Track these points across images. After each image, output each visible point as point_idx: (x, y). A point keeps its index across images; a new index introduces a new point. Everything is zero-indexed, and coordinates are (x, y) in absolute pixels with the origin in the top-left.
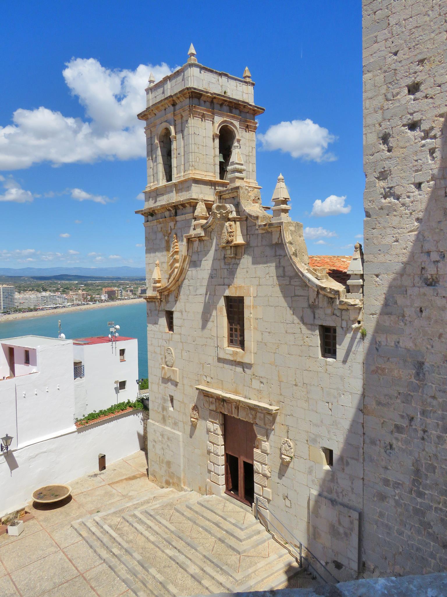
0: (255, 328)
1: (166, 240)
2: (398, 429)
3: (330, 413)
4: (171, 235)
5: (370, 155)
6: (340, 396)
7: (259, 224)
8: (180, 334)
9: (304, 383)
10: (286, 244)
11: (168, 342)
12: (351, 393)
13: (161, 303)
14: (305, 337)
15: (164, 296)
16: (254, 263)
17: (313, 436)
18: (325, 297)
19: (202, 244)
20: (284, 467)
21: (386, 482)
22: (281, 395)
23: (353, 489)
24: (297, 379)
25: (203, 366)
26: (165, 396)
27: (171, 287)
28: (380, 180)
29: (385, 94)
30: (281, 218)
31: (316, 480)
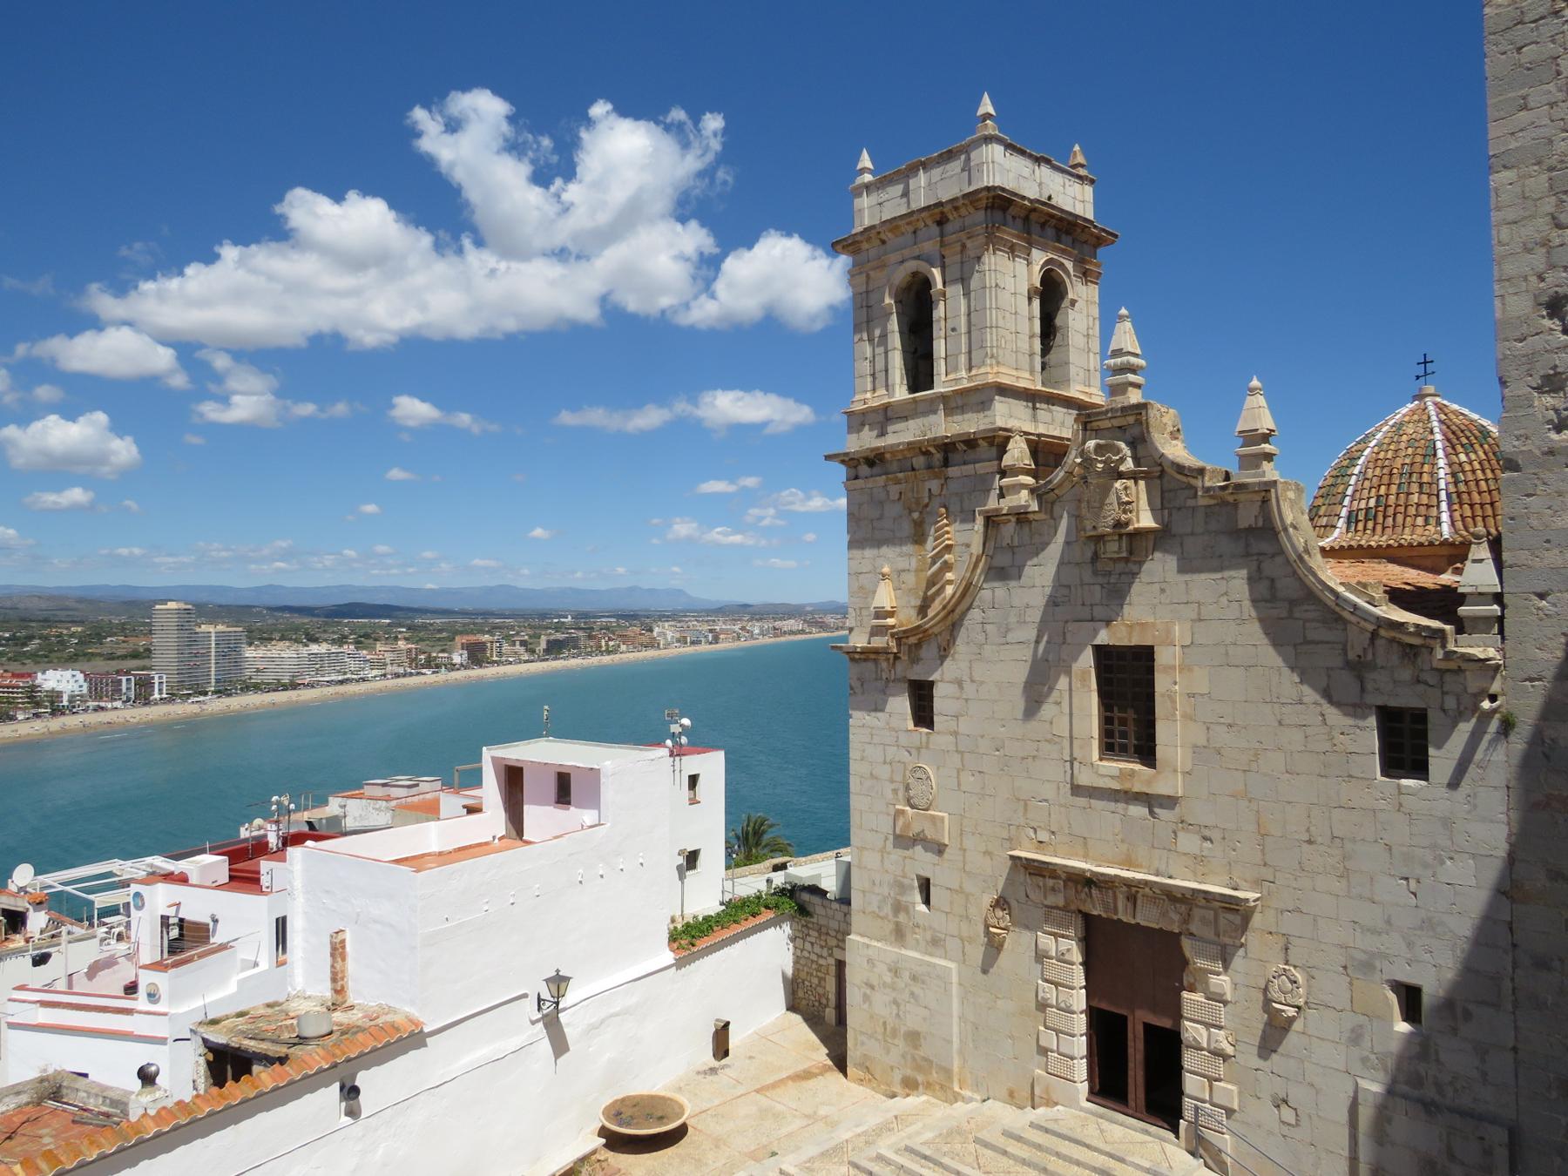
0: (1185, 716)
1: (915, 522)
3: (1413, 901)
4: (928, 509)
5: (1515, 340)
6: (1442, 863)
7: (1208, 484)
8: (955, 734)
9: (1333, 837)
10: (1285, 530)
11: (914, 752)
12: (1474, 856)
13: (894, 664)
14: (1336, 733)
15: (907, 647)
16: (1182, 570)
17: (1363, 957)
18: (1395, 645)
19: (1026, 529)
20: (1274, 1033)
22: (1265, 865)
23: (1484, 1074)
24: (1312, 828)
25: (1026, 805)
26: (904, 877)
27: (931, 627)
28: (1543, 393)
29: (1552, 214)
30: (1264, 472)
31: (1373, 1057)
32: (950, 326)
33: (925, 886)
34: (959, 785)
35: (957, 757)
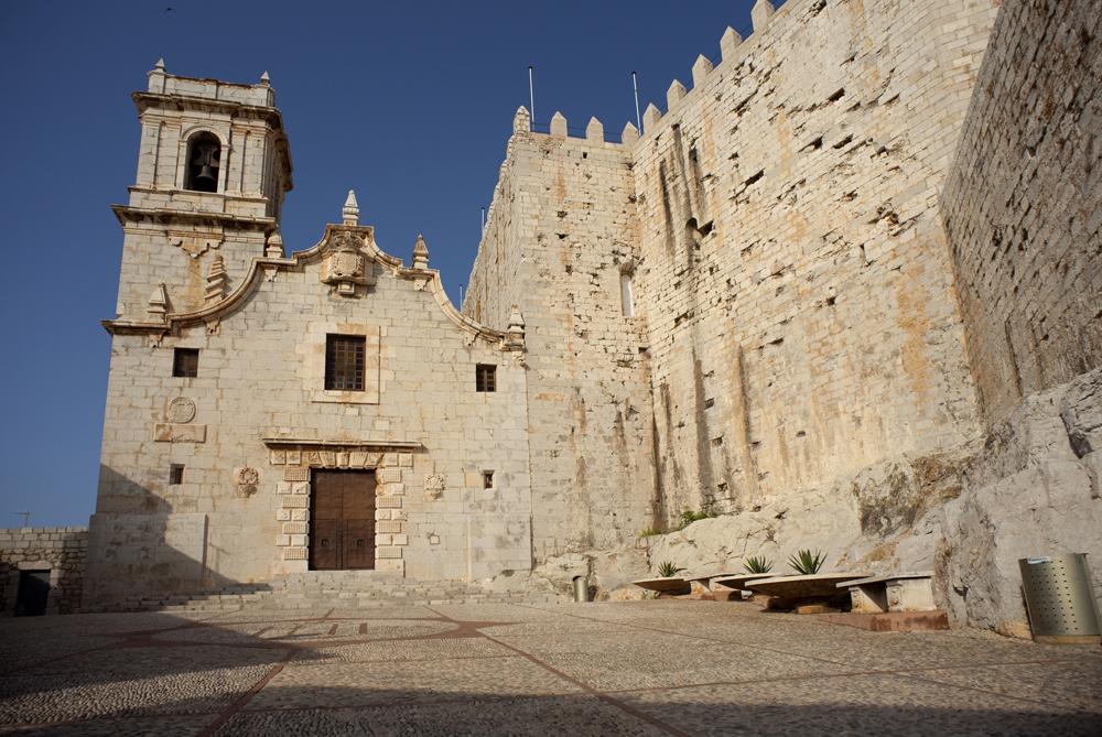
2: (563, 438)
11: (177, 390)
12: (515, 418)
19: (283, 275)
21: (554, 482)
23: (520, 499)
26: (160, 467)
32: (231, 166)
33: (177, 474)
34: (217, 408)
35: (217, 393)
